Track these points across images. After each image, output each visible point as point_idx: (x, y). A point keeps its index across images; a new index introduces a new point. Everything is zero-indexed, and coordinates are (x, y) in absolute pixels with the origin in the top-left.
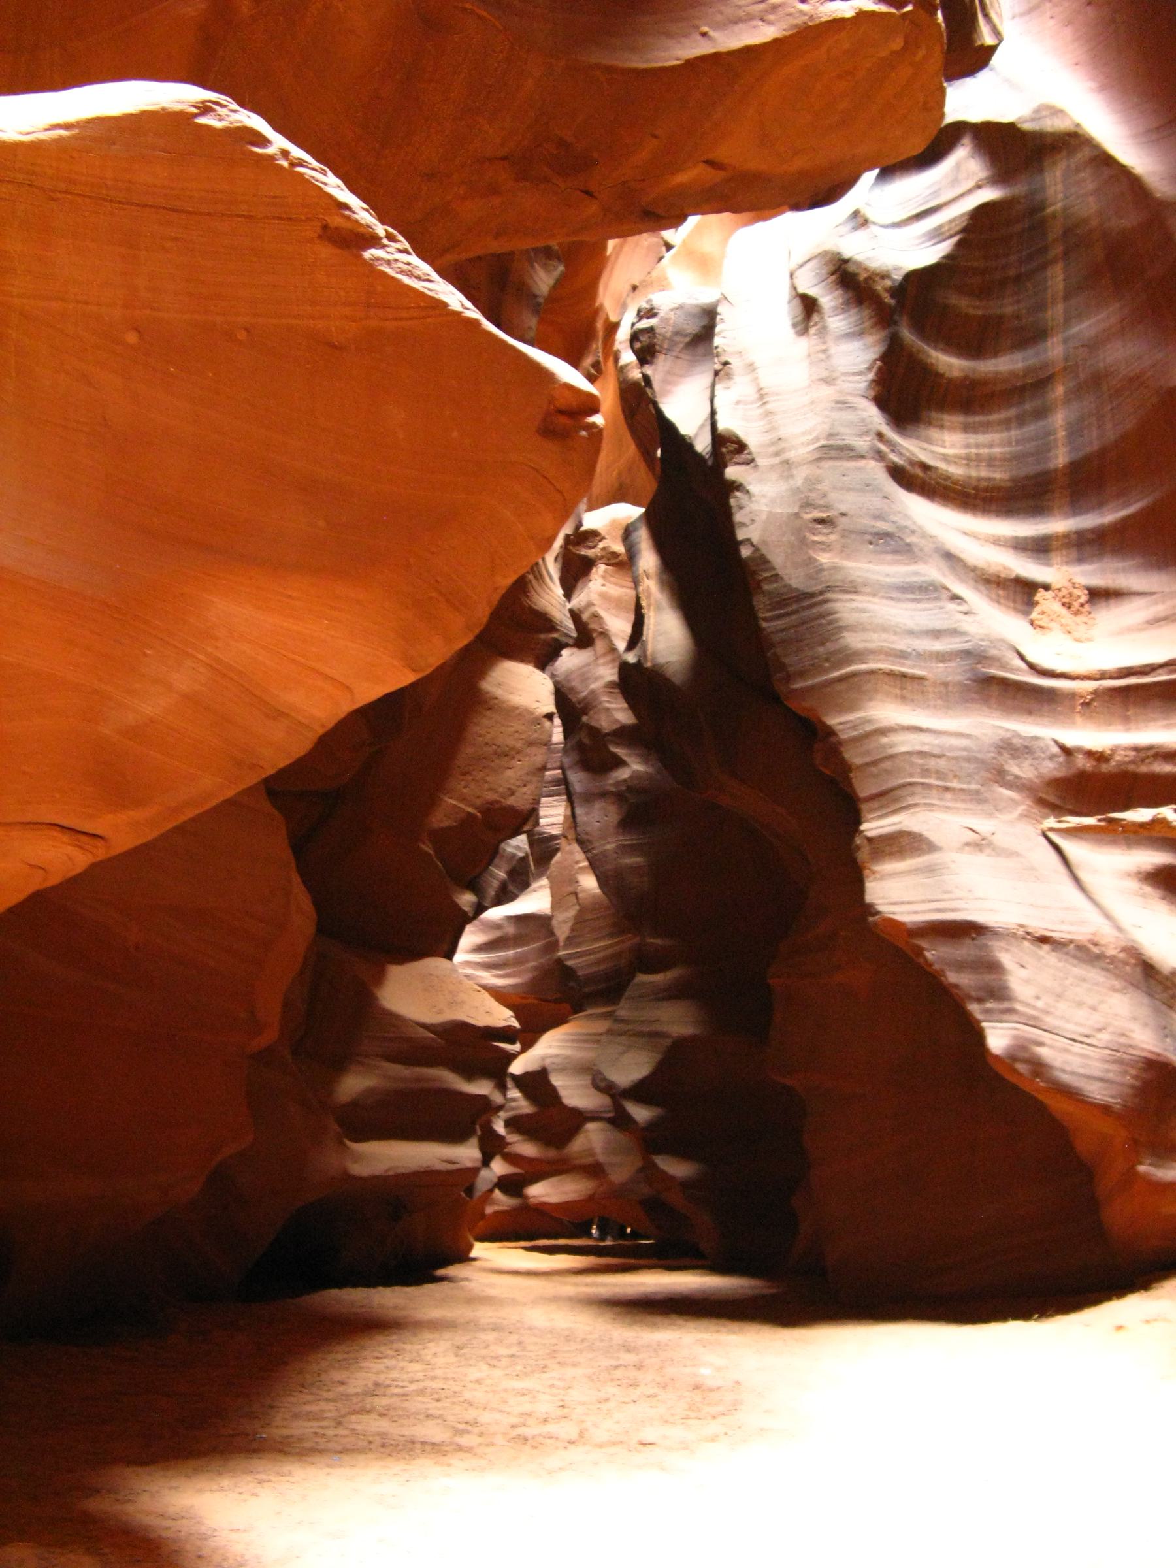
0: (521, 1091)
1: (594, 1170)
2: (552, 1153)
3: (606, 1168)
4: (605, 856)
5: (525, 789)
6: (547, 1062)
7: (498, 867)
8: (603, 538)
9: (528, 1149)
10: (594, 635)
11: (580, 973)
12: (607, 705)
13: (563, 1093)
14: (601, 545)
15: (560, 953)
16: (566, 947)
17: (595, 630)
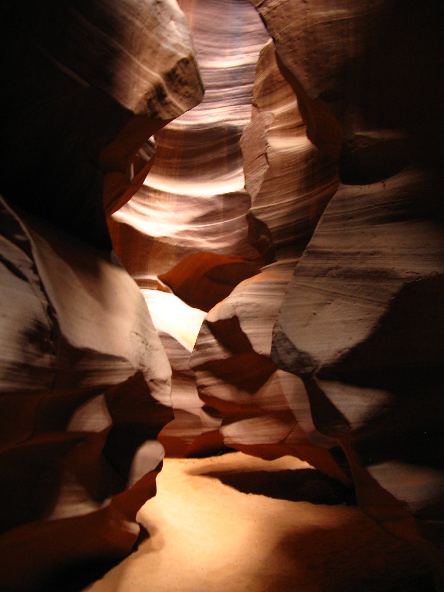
0: (216, 338)
1: (285, 417)
2: (244, 397)
3: (296, 415)
4: (288, 9)
6: (238, 311)
7: (152, 67)
9: (222, 392)
11: (270, 227)
13: (253, 340)
15: (252, 208)
16: (258, 202)
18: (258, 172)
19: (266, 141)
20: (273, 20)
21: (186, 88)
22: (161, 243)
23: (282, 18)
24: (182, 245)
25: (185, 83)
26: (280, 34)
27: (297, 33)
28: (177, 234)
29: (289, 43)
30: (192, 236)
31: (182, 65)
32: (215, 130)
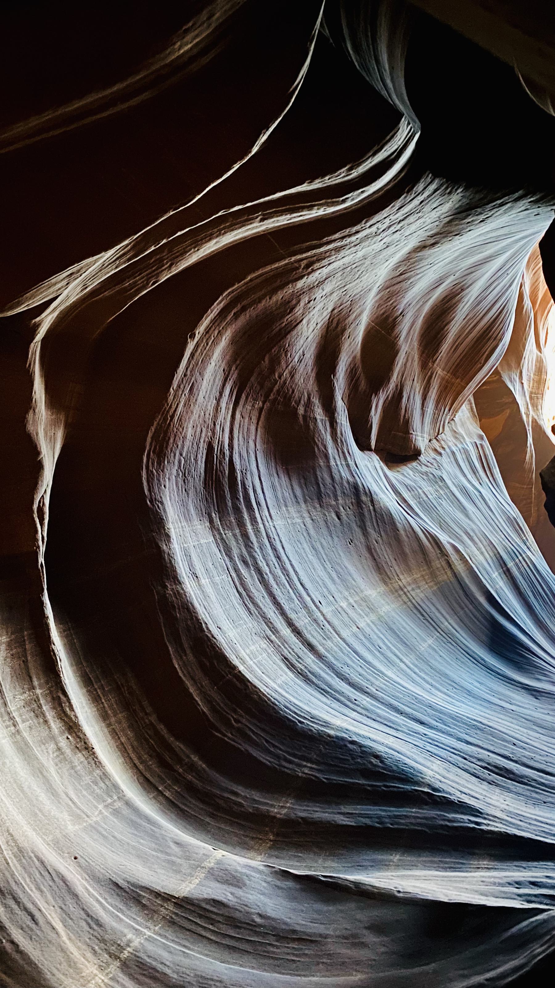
30: (66, 914)
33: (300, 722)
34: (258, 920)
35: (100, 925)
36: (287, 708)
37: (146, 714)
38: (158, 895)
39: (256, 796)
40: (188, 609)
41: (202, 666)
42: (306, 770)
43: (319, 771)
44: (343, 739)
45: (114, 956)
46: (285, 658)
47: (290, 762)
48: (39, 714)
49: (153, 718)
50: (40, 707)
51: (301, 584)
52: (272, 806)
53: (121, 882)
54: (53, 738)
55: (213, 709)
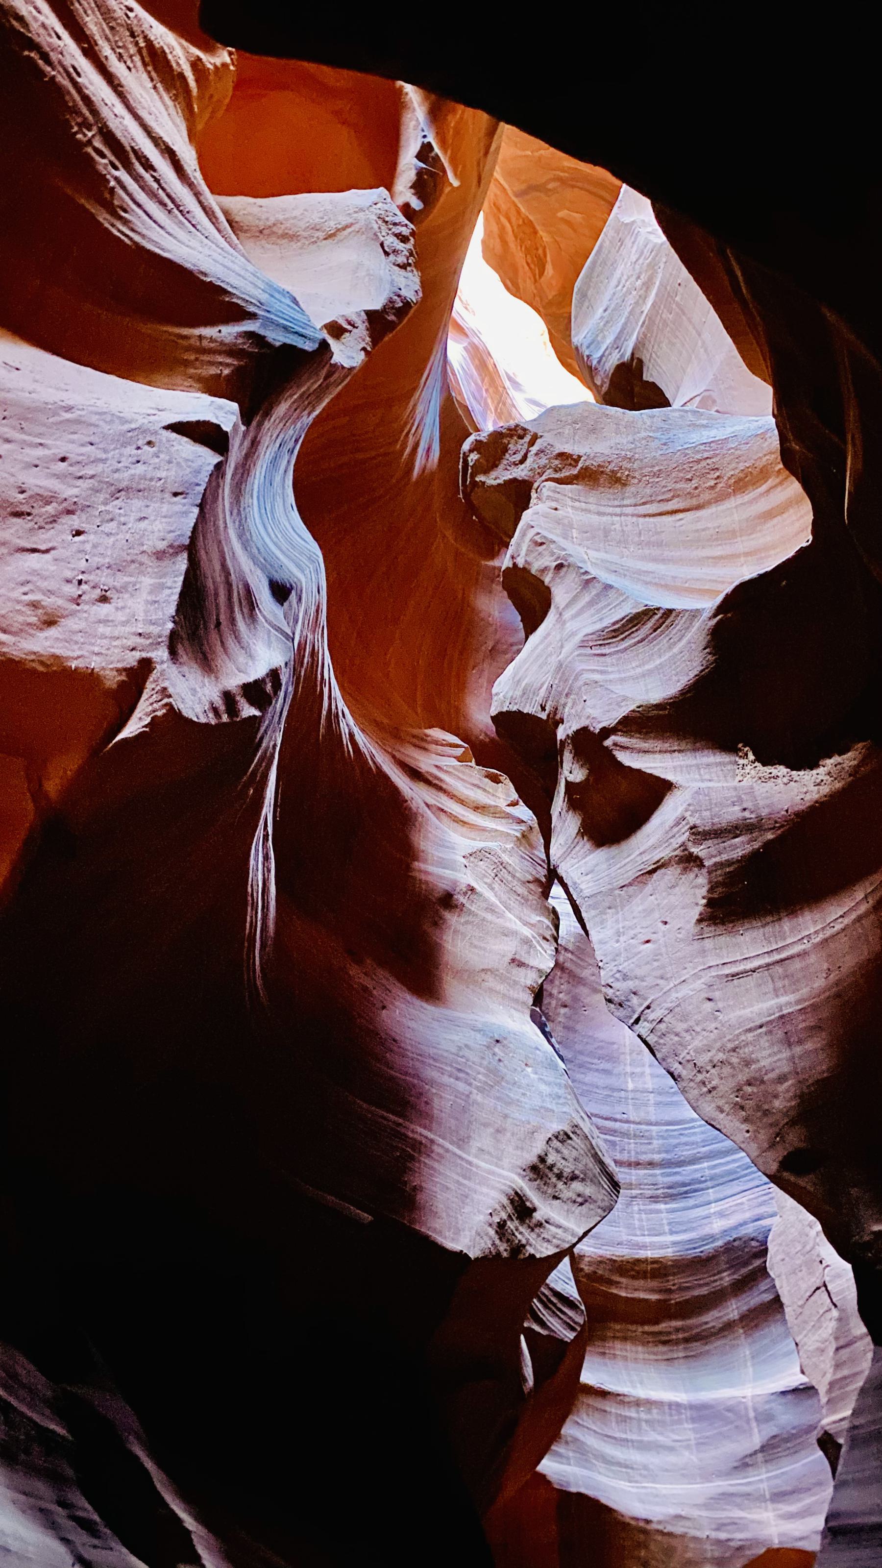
5: (104, 610)
7: (498, 1160)
8: (535, 438)
10: (547, 580)
12: (597, 677)
14: (534, 449)
17: (545, 570)
18: (820, 1328)
19: (818, 1255)
20: (662, 1041)
21: (576, 1186)
22: (670, 1534)
23: (677, 1035)
24: (723, 1536)
25: (574, 1178)
26: (680, 1063)
27: (710, 1054)
28: (706, 1506)
29: (700, 1077)
30: (740, 1507)
31: (556, 1143)
32: (736, 1244)
33: (702, 1252)
34: (794, 1431)
35: (749, 1495)
36: (687, 1250)
37: (635, 1331)
38: (751, 1455)
39: (714, 1314)
40: (601, 1262)
41: (633, 1277)
42: (726, 1279)
43: (733, 1274)
44: (729, 1243)
45: (765, 1501)
46: (651, 1197)
47: (715, 1281)
48: (625, 1419)
49: (640, 1329)
50: (621, 1415)
51: (606, 1119)
52: (728, 1314)
53: (736, 1464)
54: (639, 1420)
55: (660, 1291)
